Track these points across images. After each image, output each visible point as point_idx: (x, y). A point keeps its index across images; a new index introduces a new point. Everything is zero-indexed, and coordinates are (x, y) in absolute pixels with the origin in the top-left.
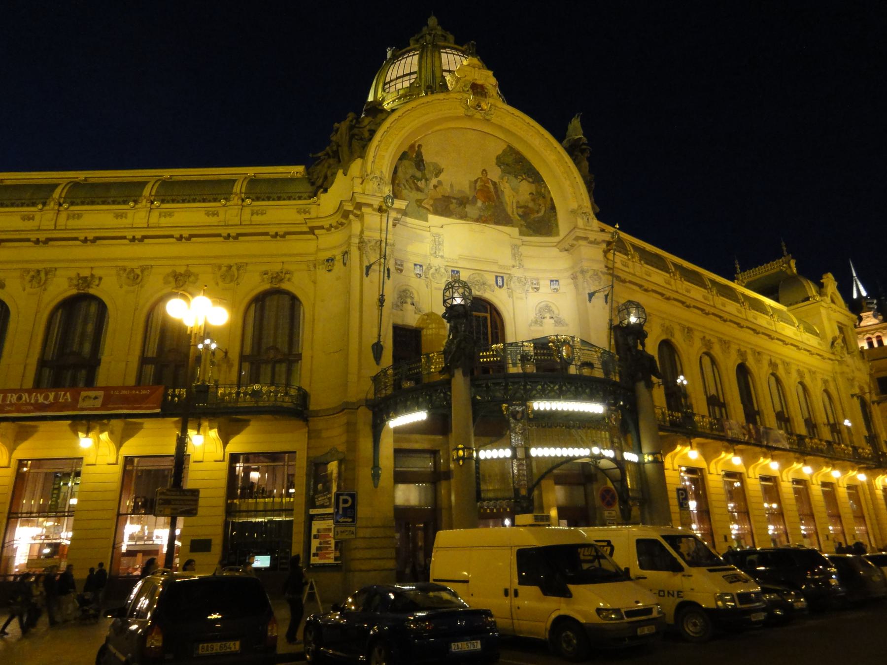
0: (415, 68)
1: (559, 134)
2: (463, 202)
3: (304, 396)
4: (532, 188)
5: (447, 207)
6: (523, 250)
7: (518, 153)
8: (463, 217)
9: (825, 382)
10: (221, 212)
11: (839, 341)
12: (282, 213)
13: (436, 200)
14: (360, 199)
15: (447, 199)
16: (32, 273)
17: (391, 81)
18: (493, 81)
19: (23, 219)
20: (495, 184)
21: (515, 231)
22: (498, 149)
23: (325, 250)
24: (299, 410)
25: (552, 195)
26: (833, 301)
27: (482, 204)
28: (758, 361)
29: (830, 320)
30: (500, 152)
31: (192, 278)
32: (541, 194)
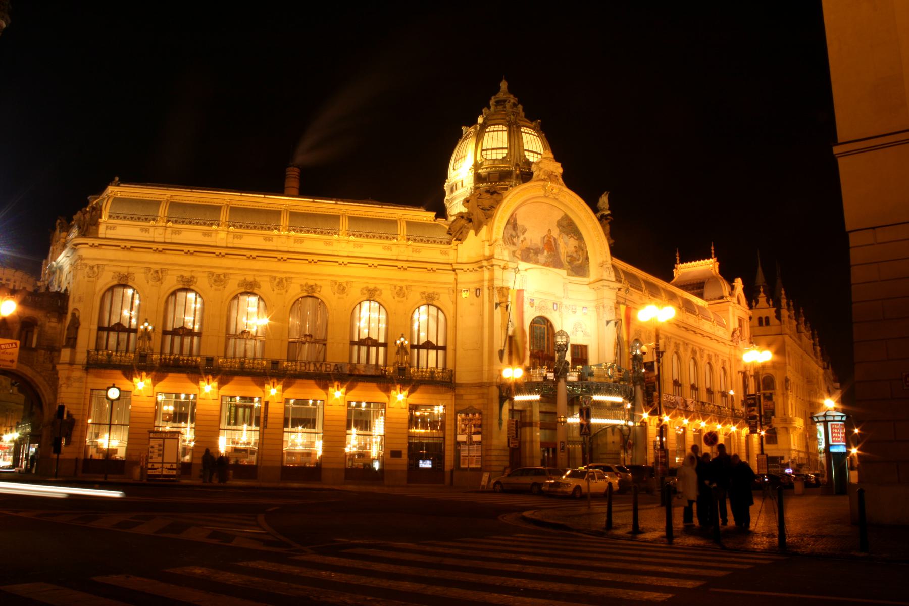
0: (506, 146)
2: (537, 252)
4: (576, 243)
5: (528, 255)
6: (570, 286)
7: (570, 219)
8: (537, 262)
9: (724, 362)
11: (738, 332)
12: (432, 253)
13: (523, 251)
15: (528, 249)
16: (277, 280)
17: (488, 150)
18: (561, 170)
19: (265, 239)
20: (555, 239)
21: (563, 272)
22: (557, 215)
23: (461, 283)
26: (739, 302)
27: (547, 254)
28: (686, 350)
29: (734, 315)
30: (559, 218)
31: (378, 293)
32: (581, 248)
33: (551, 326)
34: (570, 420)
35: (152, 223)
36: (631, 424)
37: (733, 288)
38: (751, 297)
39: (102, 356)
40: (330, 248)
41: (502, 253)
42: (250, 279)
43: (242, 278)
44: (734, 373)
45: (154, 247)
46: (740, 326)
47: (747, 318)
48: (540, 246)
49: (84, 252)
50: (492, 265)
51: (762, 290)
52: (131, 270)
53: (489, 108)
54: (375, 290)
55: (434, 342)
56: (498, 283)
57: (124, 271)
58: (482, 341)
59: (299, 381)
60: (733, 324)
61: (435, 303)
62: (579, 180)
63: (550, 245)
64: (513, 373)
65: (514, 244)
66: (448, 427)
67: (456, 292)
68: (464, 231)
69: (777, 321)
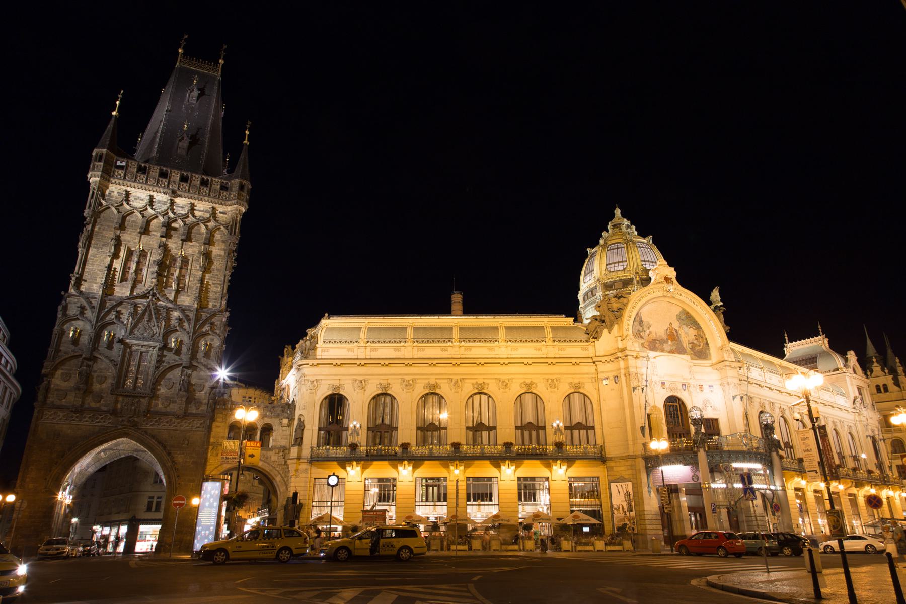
1: (706, 297)
2: (663, 342)
3: (602, 449)
5: (655, 346)
6: (695, 369)
8: (663, 351)
10: (543, 348)
11: (859, 399)
12: (574, 350)
14: (628, 353)
18: (675, 274)
21: (686, 357)
22: (677, 310)
24: (601, 458)
25: (707, 336)
27: (671, 342)
29: (852, 384)
33: (683, 403)
34: (713, 486)
35: (356, 344)
36: (772, 487)
37: (846, 360)
38: (865, 365)
39: (323, 451)
40: (493, 353)
41: (633, 346)
42: (432, 382)
43: (427, 382)
44: (862, 438)
45: (358, 362)
46: (860, 393)
47: (865, 386)
48: (665, 337)
49: (306, 370)
50: (626, 356)
51: (874, 360)
52: (341, 382)
53: (607, 231)
54: (532, 383)
55: (584, 423)
56: (632, 370)
57: (336, 383)
58: (625, 420)
59: (477, 462)
60: (853, 392)
61: (581, 390)
62: (693, 279)
63: (673, 336)
64: (660, 445)
65: (642, 337)
66: (603, 496)
67: (597, 380)
68: (599, 330)
69: (897, 388)
